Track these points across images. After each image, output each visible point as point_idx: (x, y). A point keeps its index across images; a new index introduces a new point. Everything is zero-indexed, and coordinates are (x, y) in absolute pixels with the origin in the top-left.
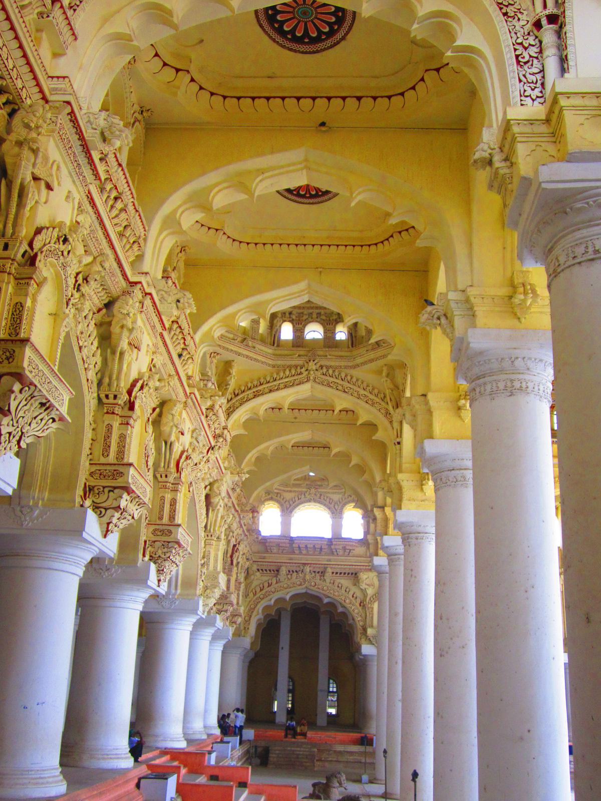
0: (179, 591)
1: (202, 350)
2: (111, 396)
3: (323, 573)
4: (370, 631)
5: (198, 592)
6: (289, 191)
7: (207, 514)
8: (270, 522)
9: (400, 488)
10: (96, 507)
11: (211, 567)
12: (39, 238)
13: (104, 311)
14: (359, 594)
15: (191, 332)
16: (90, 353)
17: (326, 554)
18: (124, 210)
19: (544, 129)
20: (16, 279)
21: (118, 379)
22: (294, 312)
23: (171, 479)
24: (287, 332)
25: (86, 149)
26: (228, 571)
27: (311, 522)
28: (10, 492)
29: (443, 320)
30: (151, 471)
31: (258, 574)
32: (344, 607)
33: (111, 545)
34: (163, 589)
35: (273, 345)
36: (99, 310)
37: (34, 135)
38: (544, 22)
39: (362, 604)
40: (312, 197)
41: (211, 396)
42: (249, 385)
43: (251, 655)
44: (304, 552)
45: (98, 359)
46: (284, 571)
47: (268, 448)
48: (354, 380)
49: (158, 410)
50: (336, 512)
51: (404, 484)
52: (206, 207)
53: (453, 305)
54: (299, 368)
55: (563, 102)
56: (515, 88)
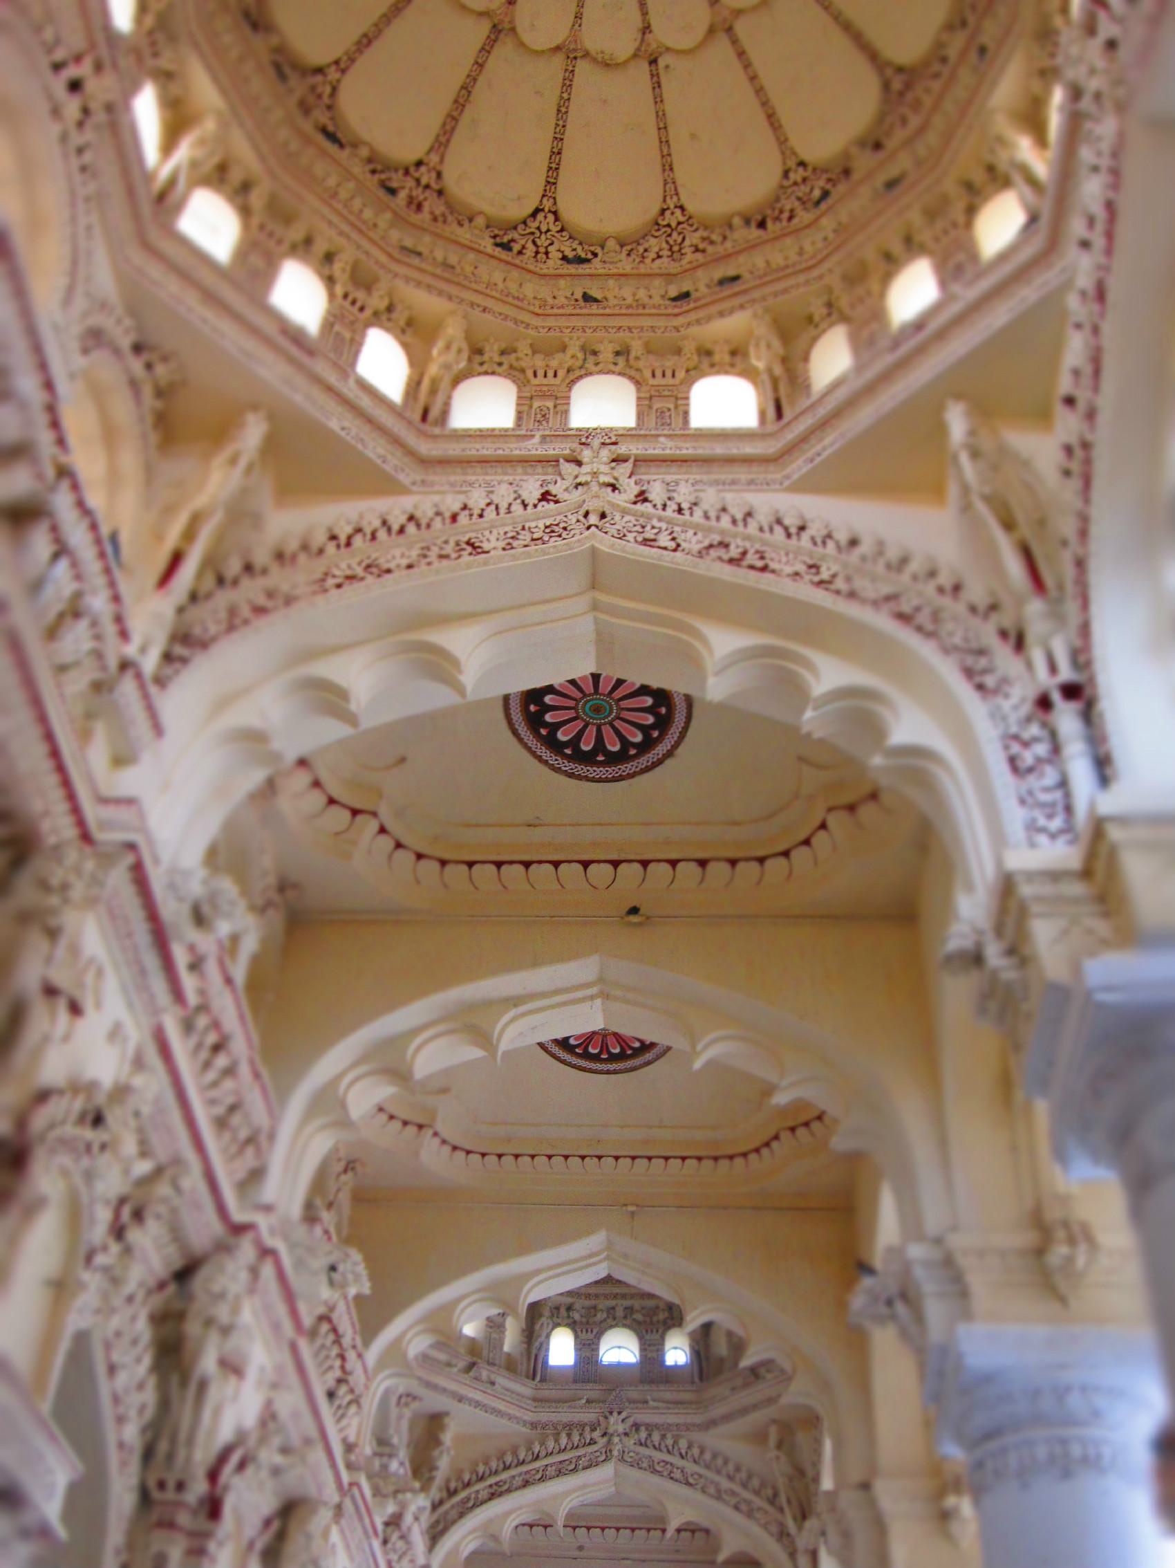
1: (383, 1384)
2: (171, 1484)
6: (563, 1043)
13: (172, 1288)
15: (359, 1341)
16: (130, 1380)
18: (230, 1071)
19: (1077, 889)
21: (190, 1441)
22: (577, 1306)
24: (561, 1349)
25: (160, 938)
29: (900, 1308)
35: (534, 1379)
36: (162, 1286)
37: (54, 900)
38: (1056, 697)
40: (613, 1058)
41: (396, 1492)
42: (481, 1469)
45: (149, 1396)
48: (707, 1456)
49: (276, 1525)
52: (399, 1074)
53: (919, 1272)
54: (587, 1429)
55: (1115, 833)
56: (1015, 817)
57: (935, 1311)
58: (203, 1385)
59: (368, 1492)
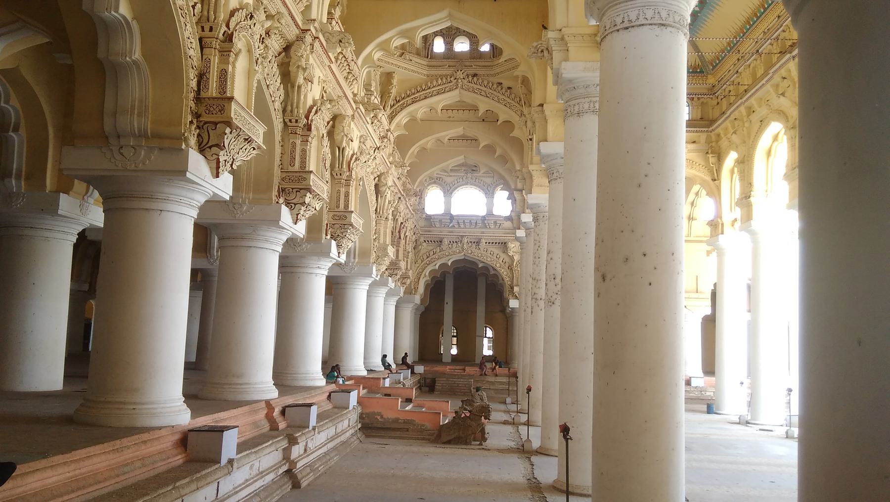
0: (357, 260)
2: (294, 121)
3: (478, 243)
4: (516, 289)
5: (372, 261)
7: (377, 200)
8: (434, 202)
9: (531, 177)
10: (287, 204)
11: (382, 241)
12: (233, 19)
14: (507, 259)
15: (355, 58)
16: (275, 92)
17: (480, 228)
20: (220, 52)
21: (297, 107)
23: (344, 177)
26: (396, 242)
27: (468, 201)
28: (228, 198)
29: (546, 53)
30: (329, 170)
31: (424, 244)
32: (494, 269)
33: (300, 229)
34: (343, 258)
36: (280, 54)
39: (510, 268)
43: (423, 309)
44: (462, 226)
45: (282, 91)
47: (428, 142)
50: (489, 193)
51: (534, 173)
53: (552, 42)
57: (557, 56)
58: (299, 87)
59: (363, 111)
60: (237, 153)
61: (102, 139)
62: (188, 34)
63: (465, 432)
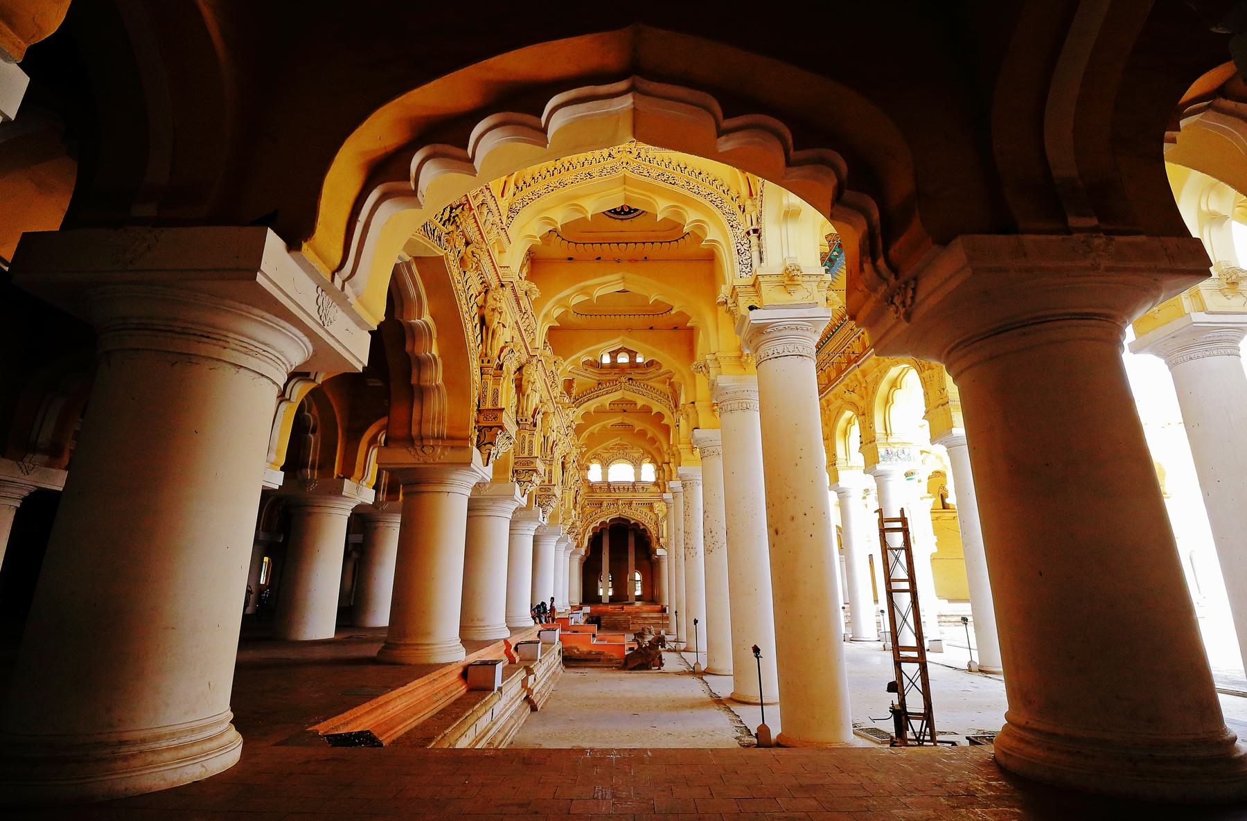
8: (595, 473)
10: (518, 481)
14: (654, 517)
19: (752, 289)
27: (621, 472)
33: (524, 501)
46: (605, 504)
50: (637, 465)
55: (760, 279)
60: (502, 447)
61: (409, 441)
62: (475, 365)
63: (644, 659)
